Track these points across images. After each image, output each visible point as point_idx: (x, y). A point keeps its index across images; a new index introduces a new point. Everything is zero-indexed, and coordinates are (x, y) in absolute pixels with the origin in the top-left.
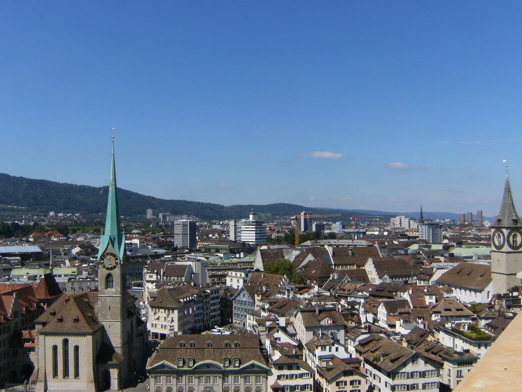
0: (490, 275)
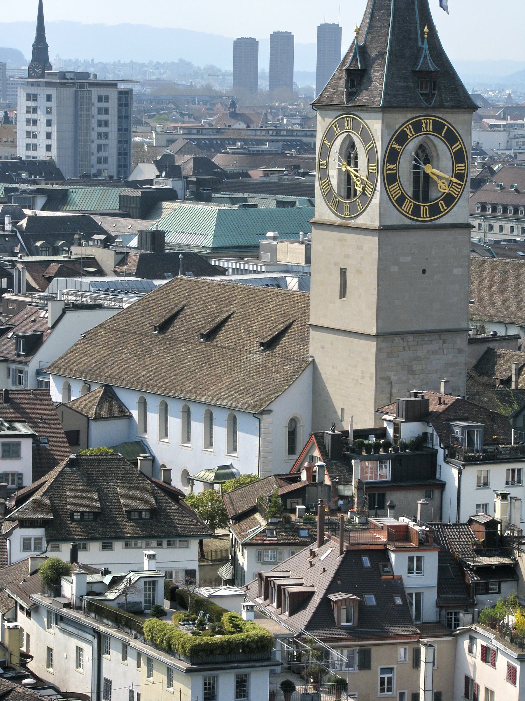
0: (305, 340)
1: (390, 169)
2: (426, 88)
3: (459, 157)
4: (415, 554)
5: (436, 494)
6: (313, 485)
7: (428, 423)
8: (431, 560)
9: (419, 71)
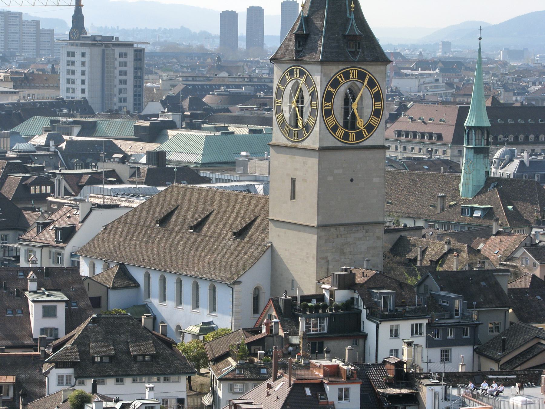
0: (265, 230)
1: (327, 106)
2: (353, 47)
3: (377, 97)
4: (344, 386)
5: (361, 342)
6: (270, 336)
7: (355, 290)
8: (355, 390)
9: (347, 35)
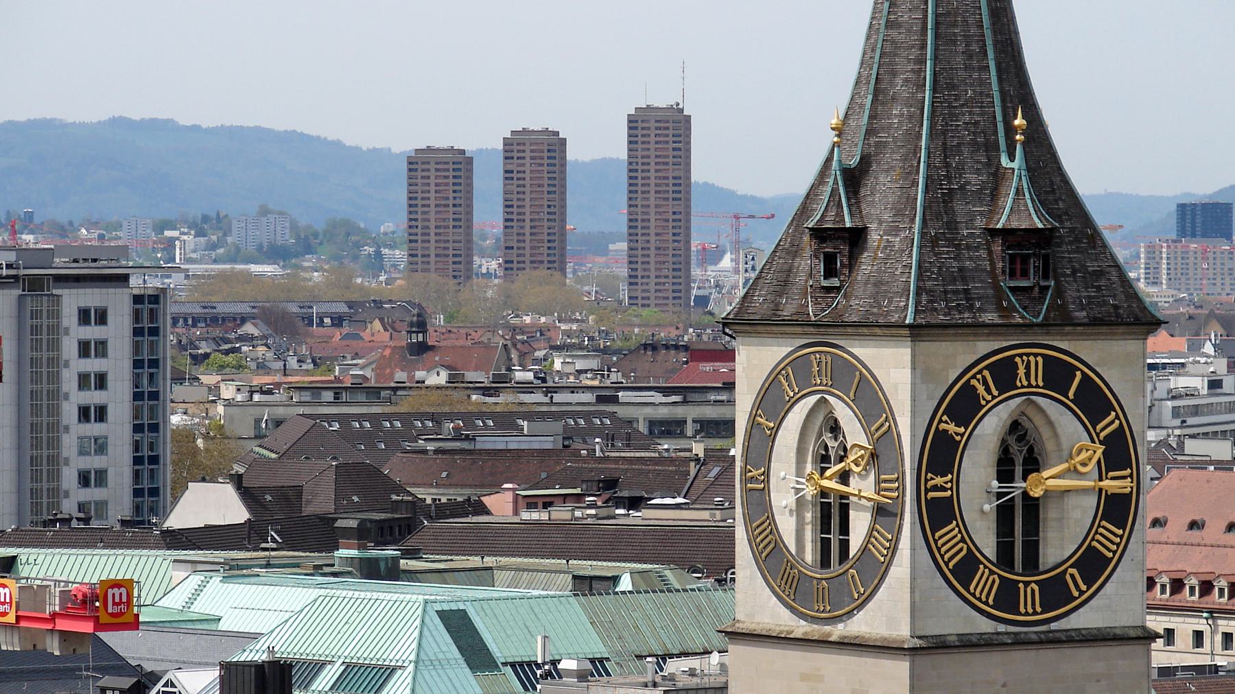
1: (935, 488)
2: (1025, 274)
3: (1118, 453)
